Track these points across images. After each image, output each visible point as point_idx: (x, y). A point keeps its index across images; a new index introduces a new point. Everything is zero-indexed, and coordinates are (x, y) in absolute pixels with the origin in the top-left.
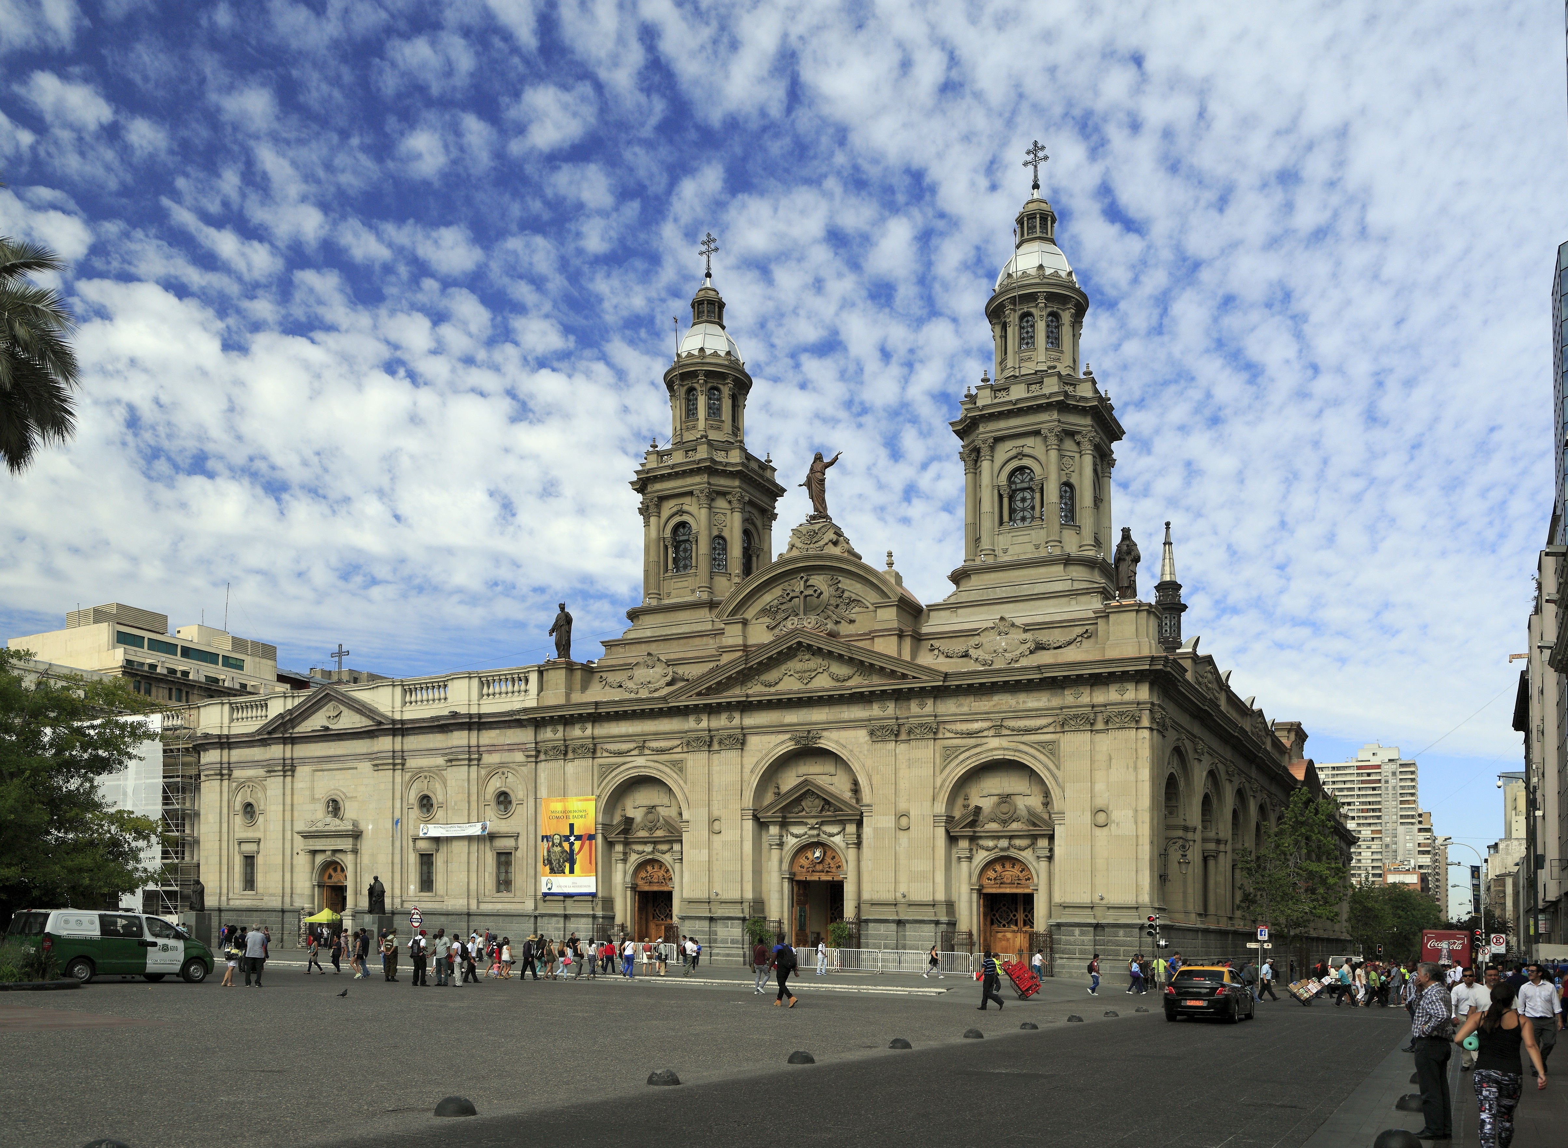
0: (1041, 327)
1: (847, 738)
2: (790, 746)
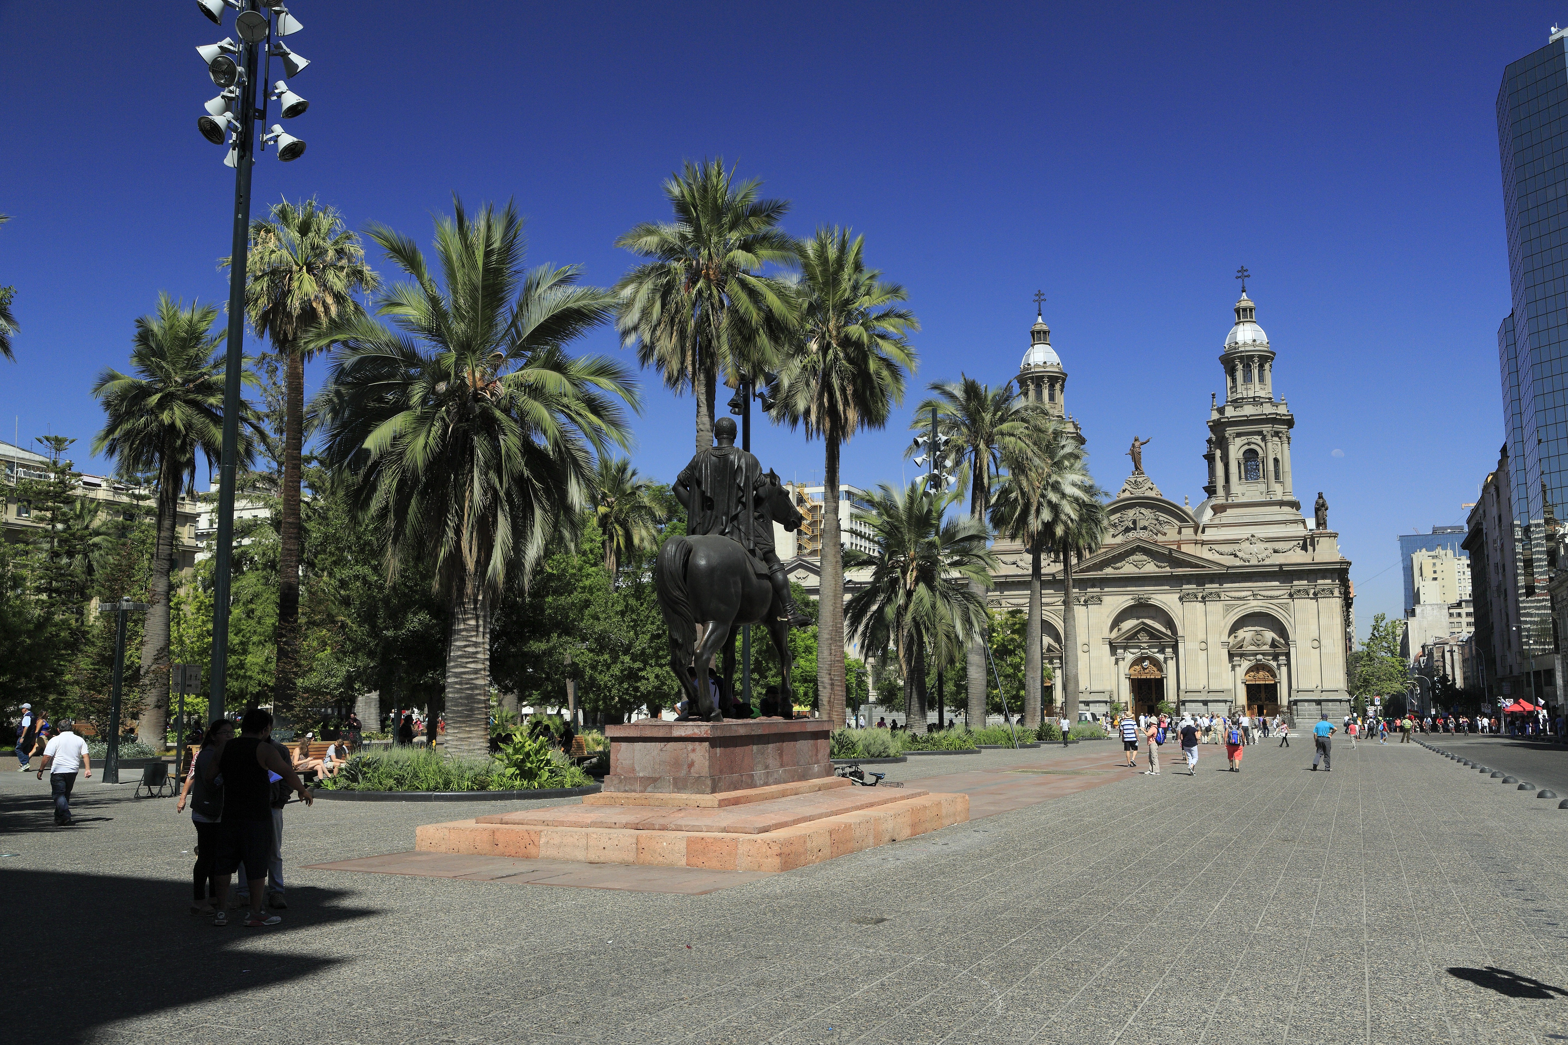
0: (1256, 372)
1: (1166, 599)
2: (1132, 603)
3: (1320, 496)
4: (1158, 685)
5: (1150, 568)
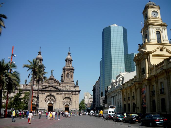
1: (54, 94)
2: (49, 94)
3: (77, 81)
4: (52, 107)
5: (52, 89)
